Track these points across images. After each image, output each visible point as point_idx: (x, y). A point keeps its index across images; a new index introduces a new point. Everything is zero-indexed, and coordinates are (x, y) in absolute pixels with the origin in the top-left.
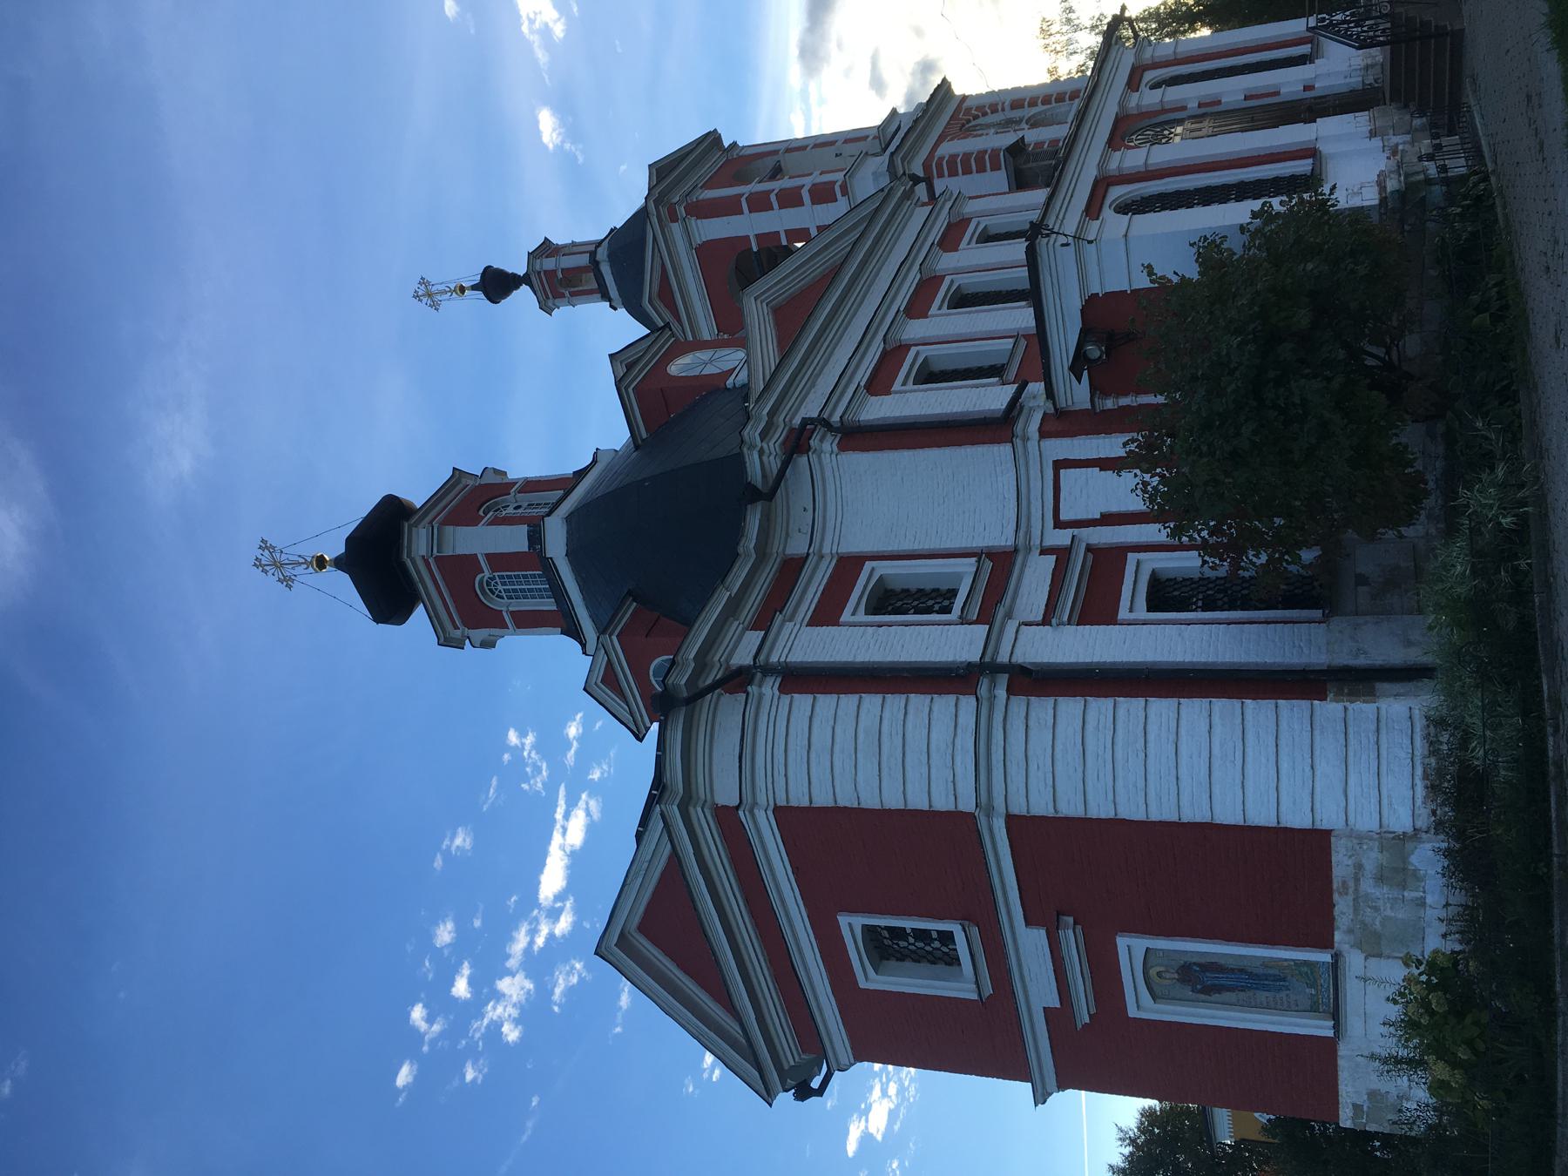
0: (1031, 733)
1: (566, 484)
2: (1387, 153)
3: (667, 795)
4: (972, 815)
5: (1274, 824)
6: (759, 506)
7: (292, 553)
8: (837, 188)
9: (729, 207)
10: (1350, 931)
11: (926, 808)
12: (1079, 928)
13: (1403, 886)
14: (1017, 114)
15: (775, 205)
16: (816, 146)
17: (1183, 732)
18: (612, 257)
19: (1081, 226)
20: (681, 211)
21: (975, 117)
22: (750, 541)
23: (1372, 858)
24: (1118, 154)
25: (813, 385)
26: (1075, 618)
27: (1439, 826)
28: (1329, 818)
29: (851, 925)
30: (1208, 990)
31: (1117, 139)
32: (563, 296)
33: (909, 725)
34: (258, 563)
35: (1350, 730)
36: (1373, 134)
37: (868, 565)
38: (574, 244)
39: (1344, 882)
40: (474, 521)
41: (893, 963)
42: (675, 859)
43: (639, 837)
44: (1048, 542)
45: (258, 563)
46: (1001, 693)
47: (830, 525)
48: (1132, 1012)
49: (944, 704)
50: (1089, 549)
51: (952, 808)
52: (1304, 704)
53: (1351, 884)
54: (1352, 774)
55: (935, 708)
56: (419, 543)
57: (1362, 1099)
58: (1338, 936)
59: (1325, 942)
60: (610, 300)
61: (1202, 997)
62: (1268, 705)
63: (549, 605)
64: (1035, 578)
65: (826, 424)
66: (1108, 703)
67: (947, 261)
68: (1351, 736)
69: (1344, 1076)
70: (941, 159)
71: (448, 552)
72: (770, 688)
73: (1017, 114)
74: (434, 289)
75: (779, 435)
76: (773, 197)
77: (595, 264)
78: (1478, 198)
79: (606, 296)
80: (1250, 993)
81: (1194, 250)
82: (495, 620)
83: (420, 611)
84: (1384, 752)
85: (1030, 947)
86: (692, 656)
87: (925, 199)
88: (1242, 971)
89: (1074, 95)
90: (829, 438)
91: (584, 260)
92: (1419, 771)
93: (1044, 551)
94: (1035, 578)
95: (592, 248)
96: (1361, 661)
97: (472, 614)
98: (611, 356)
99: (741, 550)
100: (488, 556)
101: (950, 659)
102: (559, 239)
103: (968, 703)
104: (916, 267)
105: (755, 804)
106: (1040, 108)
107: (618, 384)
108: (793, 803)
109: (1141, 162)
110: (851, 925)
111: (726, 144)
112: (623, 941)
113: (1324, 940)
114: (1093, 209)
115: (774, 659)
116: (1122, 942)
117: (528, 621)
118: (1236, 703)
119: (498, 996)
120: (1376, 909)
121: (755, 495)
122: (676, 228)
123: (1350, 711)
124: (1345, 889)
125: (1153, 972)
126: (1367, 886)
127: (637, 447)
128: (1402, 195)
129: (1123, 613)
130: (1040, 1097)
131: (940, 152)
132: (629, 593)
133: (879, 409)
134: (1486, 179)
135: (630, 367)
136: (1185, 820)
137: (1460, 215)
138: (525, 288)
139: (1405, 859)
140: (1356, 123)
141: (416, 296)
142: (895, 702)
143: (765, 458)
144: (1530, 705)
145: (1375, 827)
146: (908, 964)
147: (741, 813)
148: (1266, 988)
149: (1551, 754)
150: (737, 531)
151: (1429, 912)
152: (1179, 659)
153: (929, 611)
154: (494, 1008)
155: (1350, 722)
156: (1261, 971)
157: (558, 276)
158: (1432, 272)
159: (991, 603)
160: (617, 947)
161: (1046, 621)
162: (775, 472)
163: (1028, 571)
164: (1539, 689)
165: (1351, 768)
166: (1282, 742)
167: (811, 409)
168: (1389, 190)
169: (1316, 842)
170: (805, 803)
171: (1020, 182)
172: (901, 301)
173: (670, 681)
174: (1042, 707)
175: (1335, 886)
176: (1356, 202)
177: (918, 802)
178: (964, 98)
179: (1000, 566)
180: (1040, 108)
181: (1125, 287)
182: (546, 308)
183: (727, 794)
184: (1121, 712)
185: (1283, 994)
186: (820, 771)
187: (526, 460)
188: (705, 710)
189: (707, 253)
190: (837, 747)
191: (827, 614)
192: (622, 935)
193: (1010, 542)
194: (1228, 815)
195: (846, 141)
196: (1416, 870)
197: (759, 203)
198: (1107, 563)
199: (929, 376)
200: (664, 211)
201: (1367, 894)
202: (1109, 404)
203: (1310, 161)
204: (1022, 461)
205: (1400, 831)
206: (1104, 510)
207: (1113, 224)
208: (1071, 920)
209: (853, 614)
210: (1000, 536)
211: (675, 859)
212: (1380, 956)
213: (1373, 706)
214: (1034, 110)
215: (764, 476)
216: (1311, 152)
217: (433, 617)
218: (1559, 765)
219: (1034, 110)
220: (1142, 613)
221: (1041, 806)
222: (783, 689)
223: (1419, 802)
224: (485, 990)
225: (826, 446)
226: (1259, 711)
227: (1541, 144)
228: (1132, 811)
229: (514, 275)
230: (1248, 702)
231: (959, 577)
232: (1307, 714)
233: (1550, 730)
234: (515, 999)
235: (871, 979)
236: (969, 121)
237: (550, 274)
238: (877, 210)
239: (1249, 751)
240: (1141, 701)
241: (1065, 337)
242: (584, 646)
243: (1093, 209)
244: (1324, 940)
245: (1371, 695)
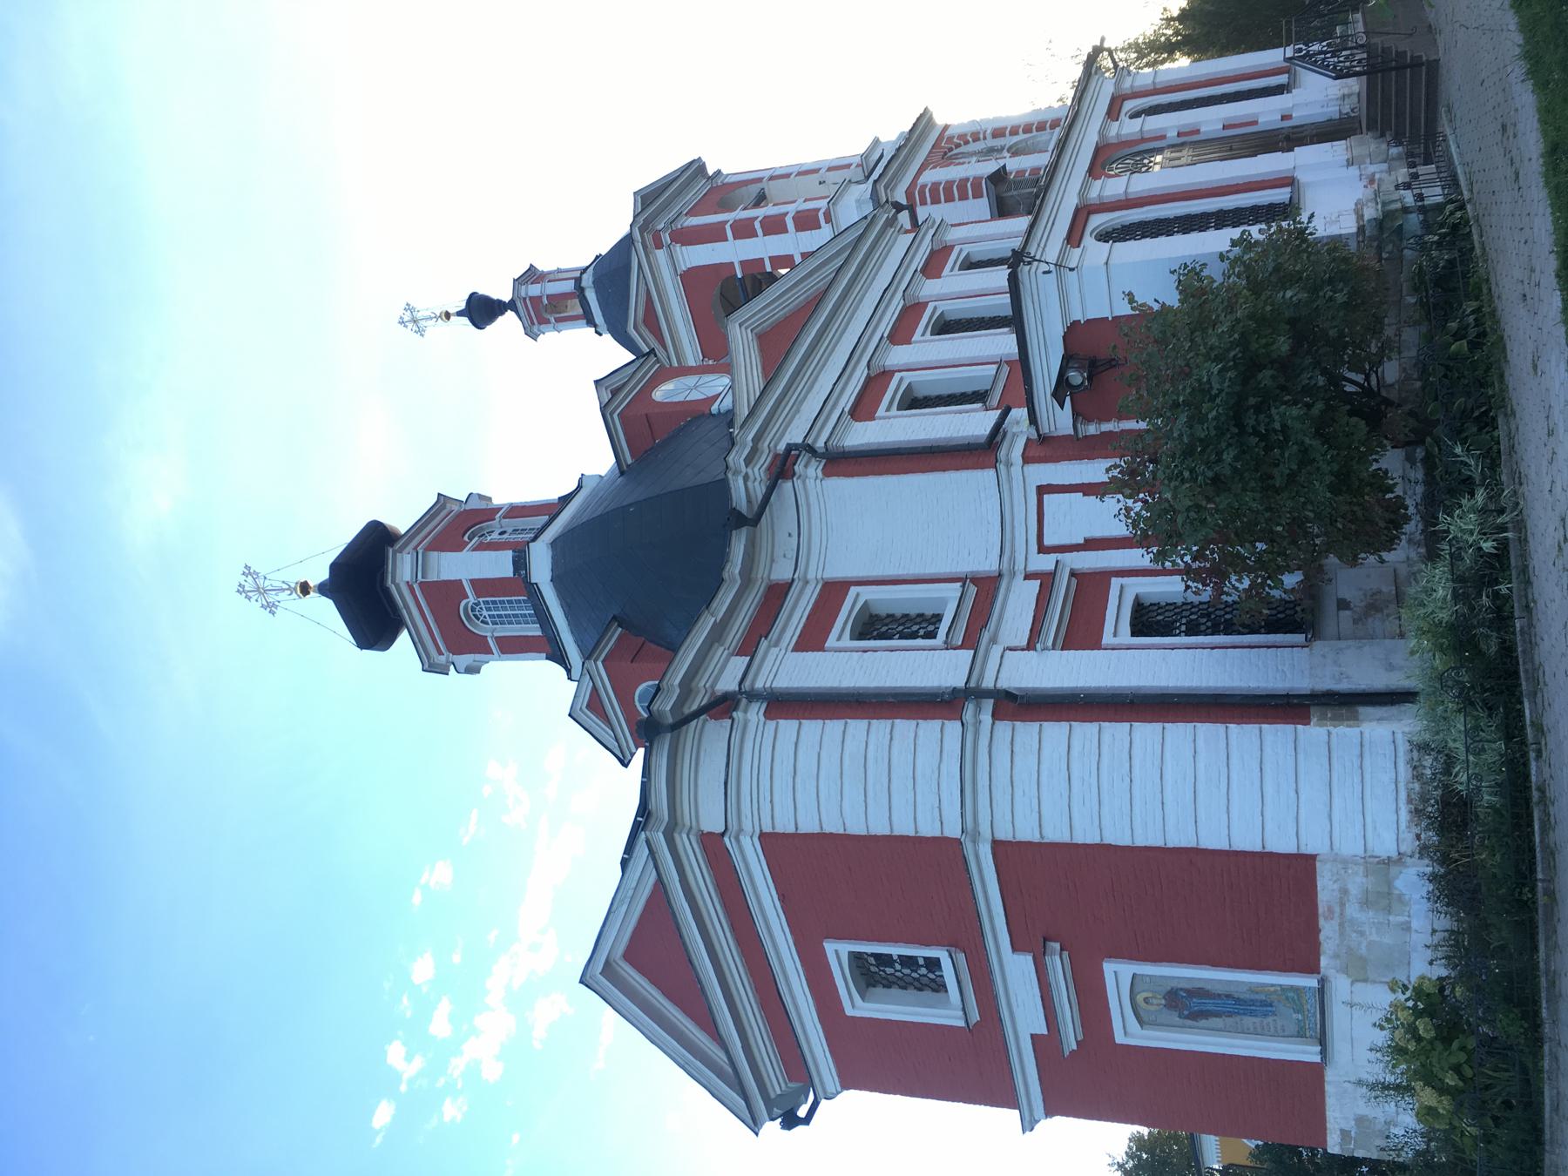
0: (1016, 759)
1: (552, 510)
2: (1365, 182)
3: (652, 821)
4: (958, 841)
5: (1258, 849)
6: (744, 530)
7: (275, 580)
9: (714, 234)
10: (1336, 956)
11: (912, 834)
12: (1065, 954)
13: (1388, 910)
14: (998, 142)
15: (760, 231)
16: (799, 174)
17: (1167, 755)
18: (598, 284)
19: (1062, 253)
20: (666, 238)
21: (958, 146)
22: (734, 568)
23: (1357, 883)
24: (1098, 183)
25: (798, 411)
26: (1060, 642)
27: (1424, 851)
28: (1312, 843)
29: (837, 952)
30: (1196, 1015)
31: (1094, 171)
32: (548, 322)
33: (895, 751)
34: (241, 590)
35: (1334, 755)
36: (1350, 163)
37: (853, 590)
38: (559, 271)
40: (459, 547)
41: (879, 990)
42: (660, 885)
43: (624, 863)
44: (1032, 568)
45: (241, 590)
46: (986, 718)
48: (1120, 1038)
49: (930, 729)
50: (1073, 574)
51: (938, 834)
52: (1288, 728)
53: (1337, 909)
54: (1337, 799)
55: (921, 733)
56: (403, 570)
57: (1350, 1125)
58: (1324, 962)
59: (1311, 967)
60: (595, 326)
61: (1189, 1022)
62: (1251, 729)
63: (534, 630)
64: (1018, 603)
65: (811, 450)
66: (1092, 728)
67: (929, 288)
68: (1334, 761)
69: (1330, 1102)
70: (923, 187)
71: (432, 577)
72: (754, 714)
73: (998, 142)
74: (419, 316)
75: (764, 460)
76: (757, 225)
77: (580, 290)
78: (1455, 227)
79: (591, 322)
80: (1238, 1018)
81: (1175, 277)
82: (479, 646)
83: (404, 639)
84: (1367, 777)
85: (1016, 974)
86: (677, 682)
87: (908, 226)
88: (1228, 996)
89: (1055, 124)
90: (814, 463)
91: (568, 286)
92: (1403, 795)
93: (1028, 577)
94: (1018, 603)
95: (578, 274)
96: (1344, 686)
97: (457, 640)
98: (596, 382)
99: (726, 575)
100: (473, 582)
101: (936, 684)
102: (543, 266)
103: (953, 727)
104: (899, 294)
105: (740, 830)
106: (1022, 136)
107: (603, 409)
108: (779, 829)
109: (1121, 190)
110: (837, 952)
111: (710, 173)
112: (608, 970)
113: (1310, 965)
114: (1074, 237)
115: (759, 685)
116: (1109, 968)
117: (513, 647)
118: (1221, 727)
120: (1362, 934)
121: (739, 520)
122: (661, 255)
123: (1334, 737)
124: (1330, 917)
125: (1140, 998)
126: (1352, 910)
127: (622, 473)
128: (1380, 224)
129: (1107, 638)
130: (1028, 1124)
131: (921, 181)
132: (614, 618)
133: (863, 435)
134: (1462, 207)
135: (615, 393)
136: (1170, 845)
137: (1439, 244)
138: (510, 314)
139: (1389, 884)
140: (1333, 152)
141: (402, 322)
142: (881, 727)
143: (750, 484)
144: (1513, 729)
145: (1361, 852)
146: (895, 991)
147: (726, 839)
148: (1252, 1014)
149: (1533, 779)
150: (722, 558)
151: (1414, 936)
152: (1163, 683)
153: (914, 636)
155: (1333, 746)
156: (1247, 996)
157: (541, 303)
158: (1412, 300)
159: (977, 626)
160: (602, 975)
161: (1030, 646)
162: (760, 497)
163: (1012, 596)
164: (1521, 713)
165: (1335, 793)
166: (1267, 768)
167: (795, 435)
168: (1366, 218)
169: (1301, 868)
170: (791, 829)
171: (1002, 209)
172: (885, 327)
173: (655, 707)
174: (1027, 732)
175: (1320, 911)
176: (1334, 230)
177: (904, 828)
178: (946, 127)
179: (984, 591)
180: (1022, 136)
181: (1106, 313)
182: (531, 334)
183: (712, 822)
184: (1106, 737)
185: (1270, 1019)
186: (806, 798)
187: (510, 487)
188: (690, 735)
189: (692, 279)
190: (822, 773)
191: (812, 639)
192: (607, 963)
193: (995, 567)
194: (1213, 840)
195: (829, 169)
196: (1400, 897)
197: (744, 230)
198: (1091, 587)
199: (913, 401)
202: (1092, 429)
203: (1288, 189)
204: (1005, 487)
205: (1384, 855)
206: (1088, 535)
207: (1094, 251)
208: (1057, 946)
209: (839, 639)
210: (987, 564)
211: (660, 885)
212: (1365, 981)
213: (1357, 730)
214: (1015, 139)
215: (749, 501)
216: (1289, 181)
217: (418, 643)
218: (1542, 790)
219: (1015, 139)
220: (1125, 636)
221: (1027, 832)
222: (769, 715)
223: (1403, 825)
225: (811, 471)
226: (1243, 735)
227: (1517, 175)
228: (1117, 836)
229: (500, 302)
230: (1232, 726)
231: (944, 602)
232: (1291, 738)
233: (1532, 755)
235: (857, 1007)
236: (951, 150)
237: (536, 300)
238: (860, 238)
239: (1234, 776)
240: (1127, 725)
241: (1047, 364)
242: (569, 671)
243: (1074, 237)
244: (1310, 965)
245: (1354, 719)
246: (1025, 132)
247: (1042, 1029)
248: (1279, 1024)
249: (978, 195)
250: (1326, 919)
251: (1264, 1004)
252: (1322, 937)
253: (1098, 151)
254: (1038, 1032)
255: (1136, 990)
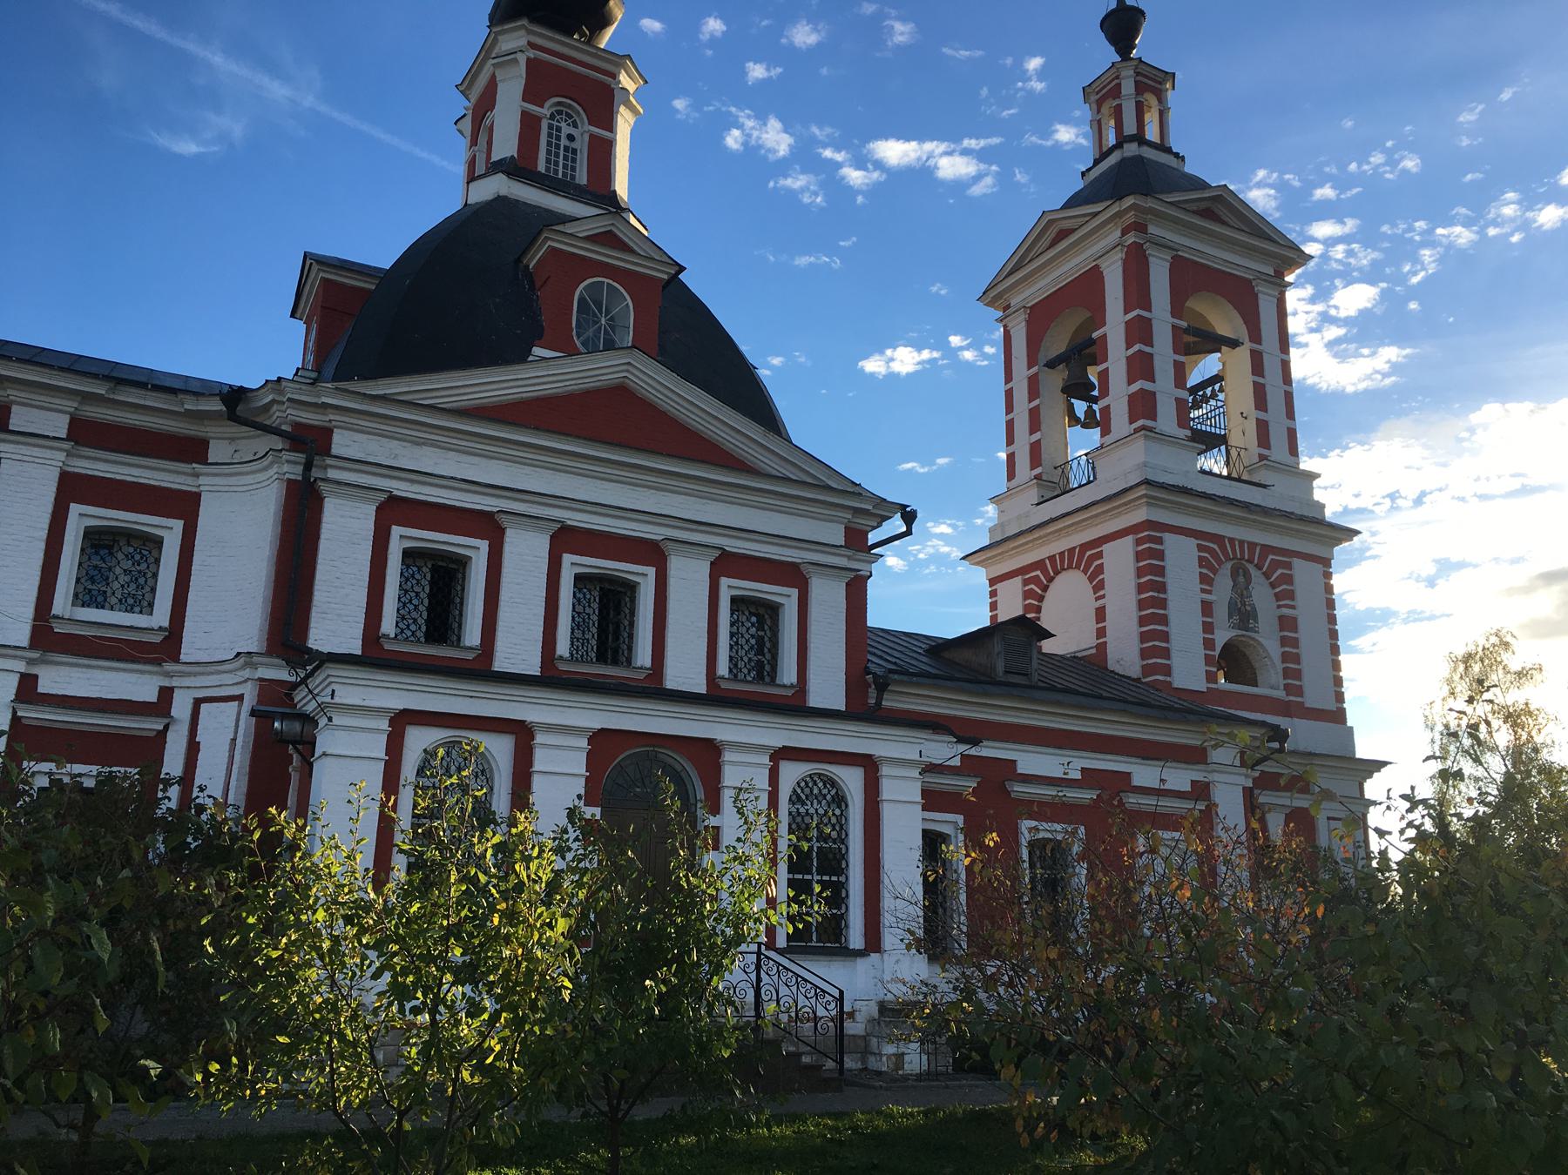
8: (1149, 423)
9: (1138, 293)
20: (1131, 239)
47: (233, 480)
70: (1160, 541)
119: (762, 118)
154: (749, 117)
178: (1326, 562)
189: (1092, 280)
197: (1139, 331)
200: (1130, 218)
224: (764, 102)
234: (765, 136)
246: (1285, 657)
249: (1027, 608)
253: (709, 743)
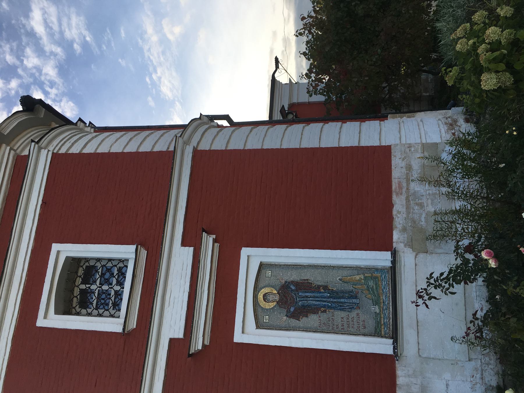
39: (400, 183)
53: (405, 185)
58: (396, 236)
61: (293, 322)
88: (325, 288)
120: (421, 205)
145: (419, 141)
175: (394, 187)
185: (354, 314)
201: (415, 193)
223: (443, 131)
247: (180, 334)
248: (362, 318)
250: (397, 194)
251: (353, 295)
252: (394, 212)
254: (176, 336)
255: (261, 285)
